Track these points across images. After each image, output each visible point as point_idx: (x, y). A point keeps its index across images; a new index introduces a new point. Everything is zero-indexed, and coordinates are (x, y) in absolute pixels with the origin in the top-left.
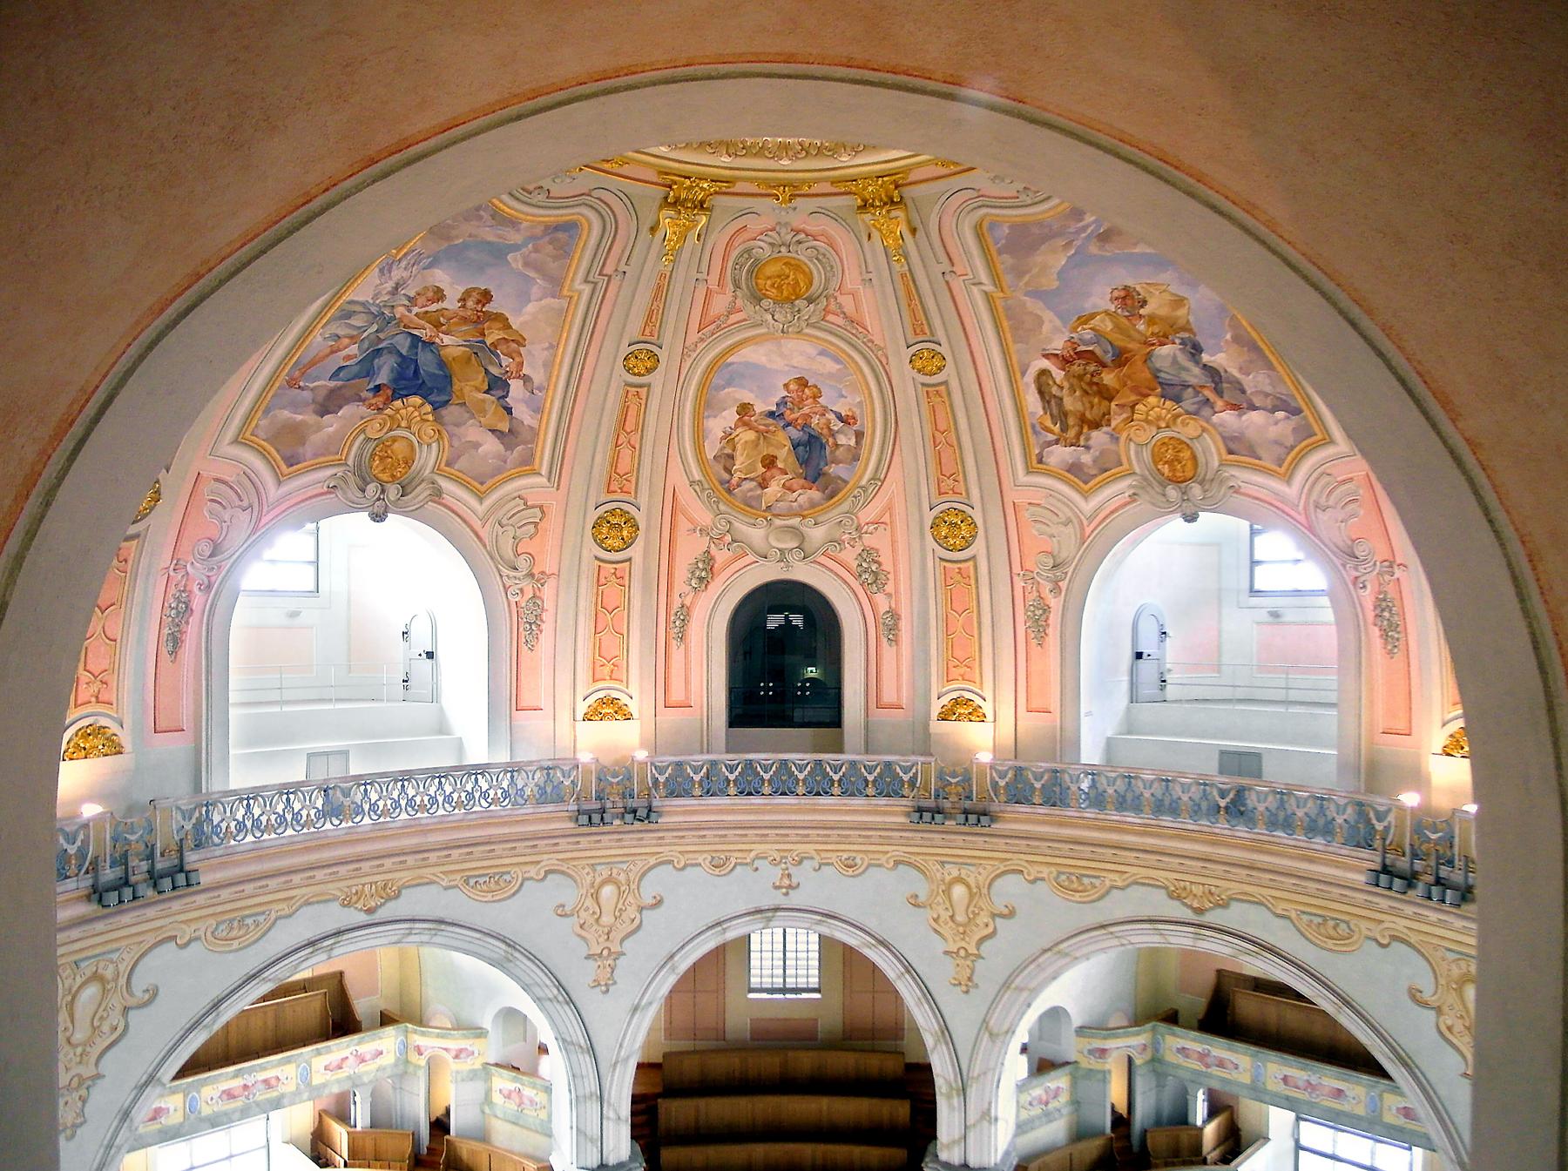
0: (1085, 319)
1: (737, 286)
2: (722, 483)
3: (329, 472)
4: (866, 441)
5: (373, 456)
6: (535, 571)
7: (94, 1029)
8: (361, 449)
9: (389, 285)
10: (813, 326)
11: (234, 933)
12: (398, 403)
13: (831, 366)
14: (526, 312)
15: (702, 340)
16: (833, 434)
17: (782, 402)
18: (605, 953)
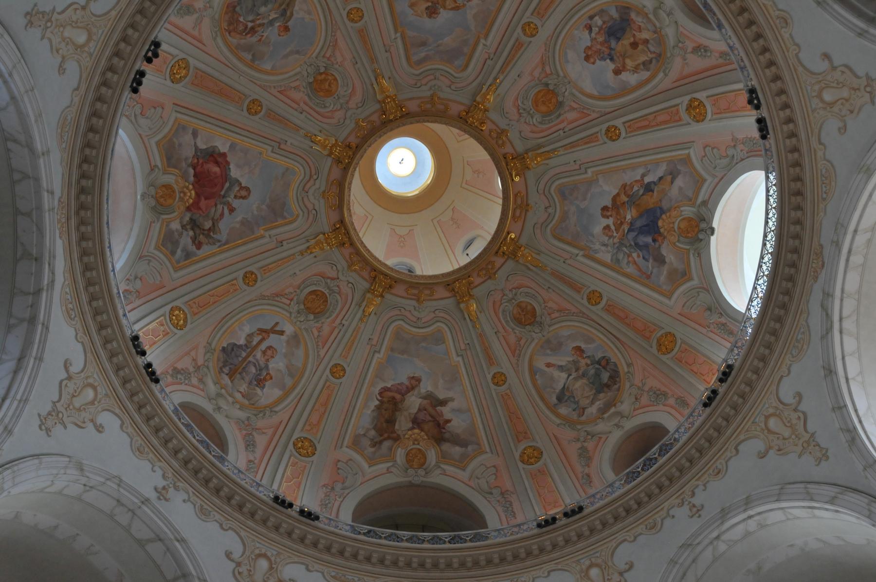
0: (456, 8)
1: (560, 115)
2: (658, 61)
3: (691, 255)
4: (591, 13)
5: (686, 237)
6: (732, 144)
7: (790, 427)
8: (682, 243)
9: (603, 248)
10: (558, 76)
11: (800, 346)
12: (662, 230)
13: (571, 55)
14: (607, 190)
15: (594, 111)
16: (601, 28)
17: (603, 59)
18: (868, 89)
